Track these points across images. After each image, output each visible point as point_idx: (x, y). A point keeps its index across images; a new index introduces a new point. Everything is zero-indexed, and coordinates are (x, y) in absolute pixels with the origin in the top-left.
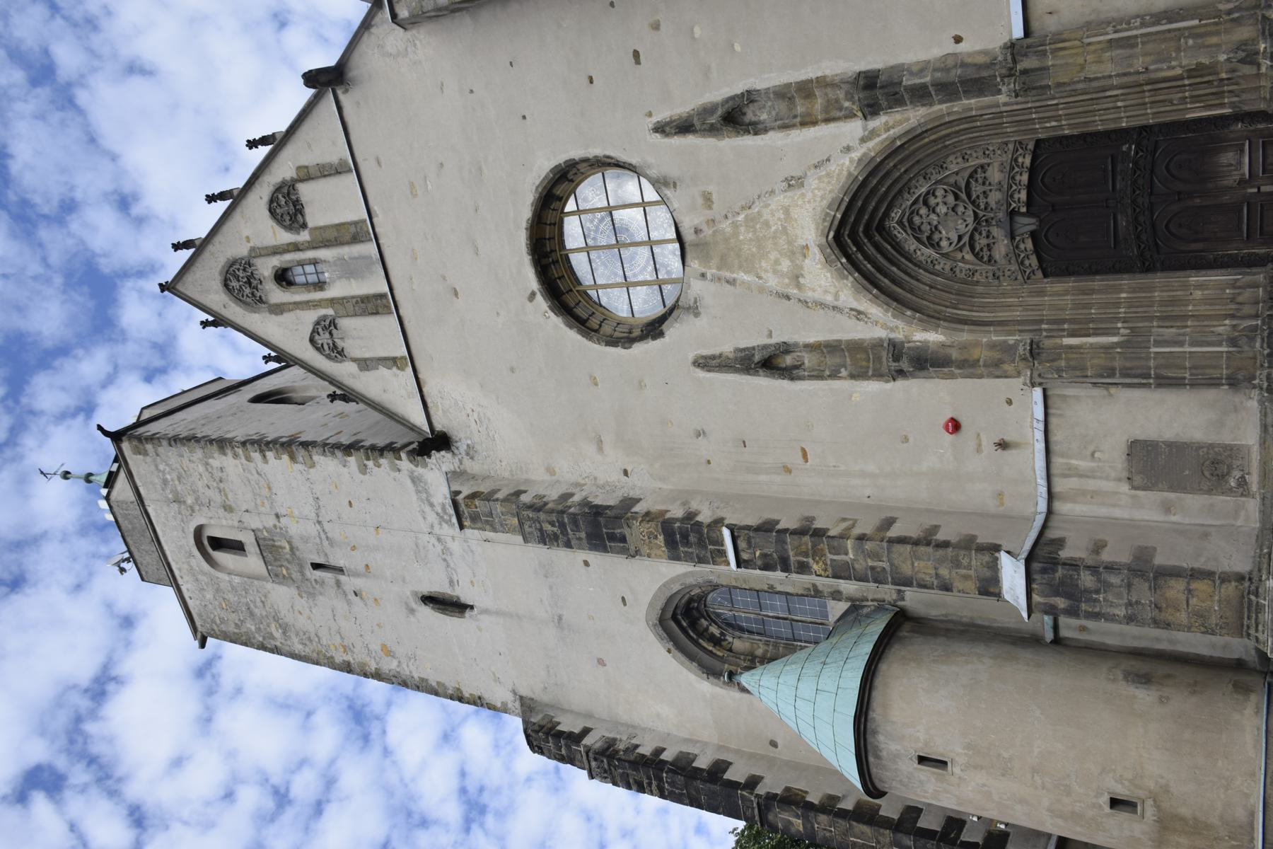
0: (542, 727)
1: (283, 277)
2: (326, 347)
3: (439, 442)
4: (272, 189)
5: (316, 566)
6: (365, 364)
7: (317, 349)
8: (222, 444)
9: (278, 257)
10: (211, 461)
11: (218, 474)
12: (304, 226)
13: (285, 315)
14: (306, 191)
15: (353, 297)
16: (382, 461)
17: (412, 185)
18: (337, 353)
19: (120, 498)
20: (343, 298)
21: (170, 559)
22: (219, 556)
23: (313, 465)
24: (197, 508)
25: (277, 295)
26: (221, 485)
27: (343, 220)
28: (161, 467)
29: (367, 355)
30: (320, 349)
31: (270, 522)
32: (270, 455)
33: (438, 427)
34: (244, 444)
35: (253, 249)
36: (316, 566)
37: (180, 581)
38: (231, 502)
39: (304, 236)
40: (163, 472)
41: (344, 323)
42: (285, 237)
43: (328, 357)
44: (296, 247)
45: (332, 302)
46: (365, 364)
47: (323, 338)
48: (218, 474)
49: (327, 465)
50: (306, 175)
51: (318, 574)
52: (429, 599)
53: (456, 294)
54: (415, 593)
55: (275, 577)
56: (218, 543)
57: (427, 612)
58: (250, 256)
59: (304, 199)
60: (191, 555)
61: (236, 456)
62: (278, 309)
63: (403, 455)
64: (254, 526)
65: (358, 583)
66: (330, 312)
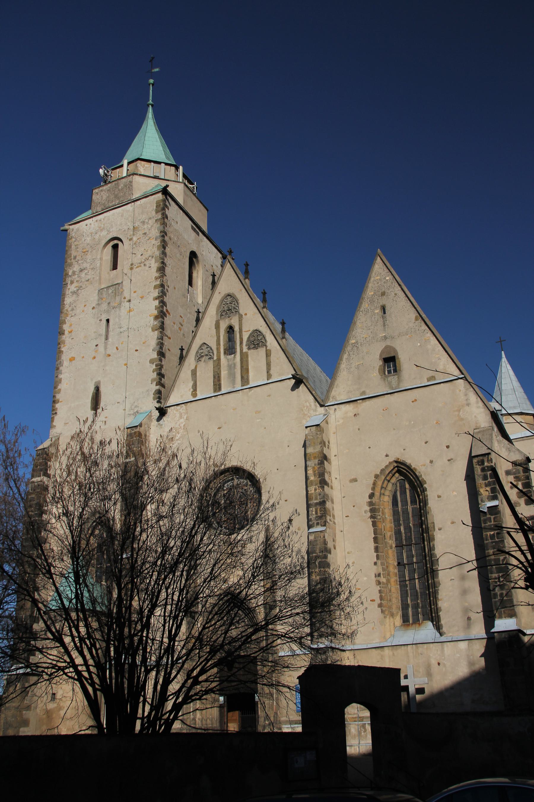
0: (48, 455)
1: (230, 329)
2: (202, 351)
3: (162, 412)
4: (264, 333)
5: (108, 321)
6: (194, 373)
7: (201, 347)
8: (162, 269)
9: (238, 330)
10: (154, 260)
11: (147, 263)
12: (249, 349)
13: (215, 330)
14: (262, 351)
15: (220, 371)
16: (155, 373)
17: (259, 412)
18: (199, 358)
19: (134, 185)
20: (220, 366)
21: (105, 214)
22: (109, 247)
23: (153, 330)
24: (131, 242)
25: (223, 326)
26: (142, 265)
27: (250, 371)
28: (150, 222)
29: (198, 374)
30: (201, 348)
31: (126, 294)
32: (157, 303)
33: (169, 410)
34: (162, 286)
35: (242, 315)
36: (108, 321)
37: (95, 219)
38: (135, 270)
39: (245, 349)
40: (148, 223)
41: (211, 362)
42: (245, 337)
43: (197, 352)
44: (241, 343)
45: (219, 359)
46: (194, 373)
47: (205, 351)
48: (147, 263)
49: (153, 337)
50: (268, 354)
51: (104, 322)
52: (97, 390)
53: (219, 428)
54: (99, 382)
55: (100, 291)
56: (115, 247)
57: (91, 390)
58: (239, 314)
59: (259, 349)
60: (109, 232)
61: (156, 278)
62: (217, 326)
63: (158, 387)
64: (124, 283)
65: (101, 348)
66: (215, 358)
